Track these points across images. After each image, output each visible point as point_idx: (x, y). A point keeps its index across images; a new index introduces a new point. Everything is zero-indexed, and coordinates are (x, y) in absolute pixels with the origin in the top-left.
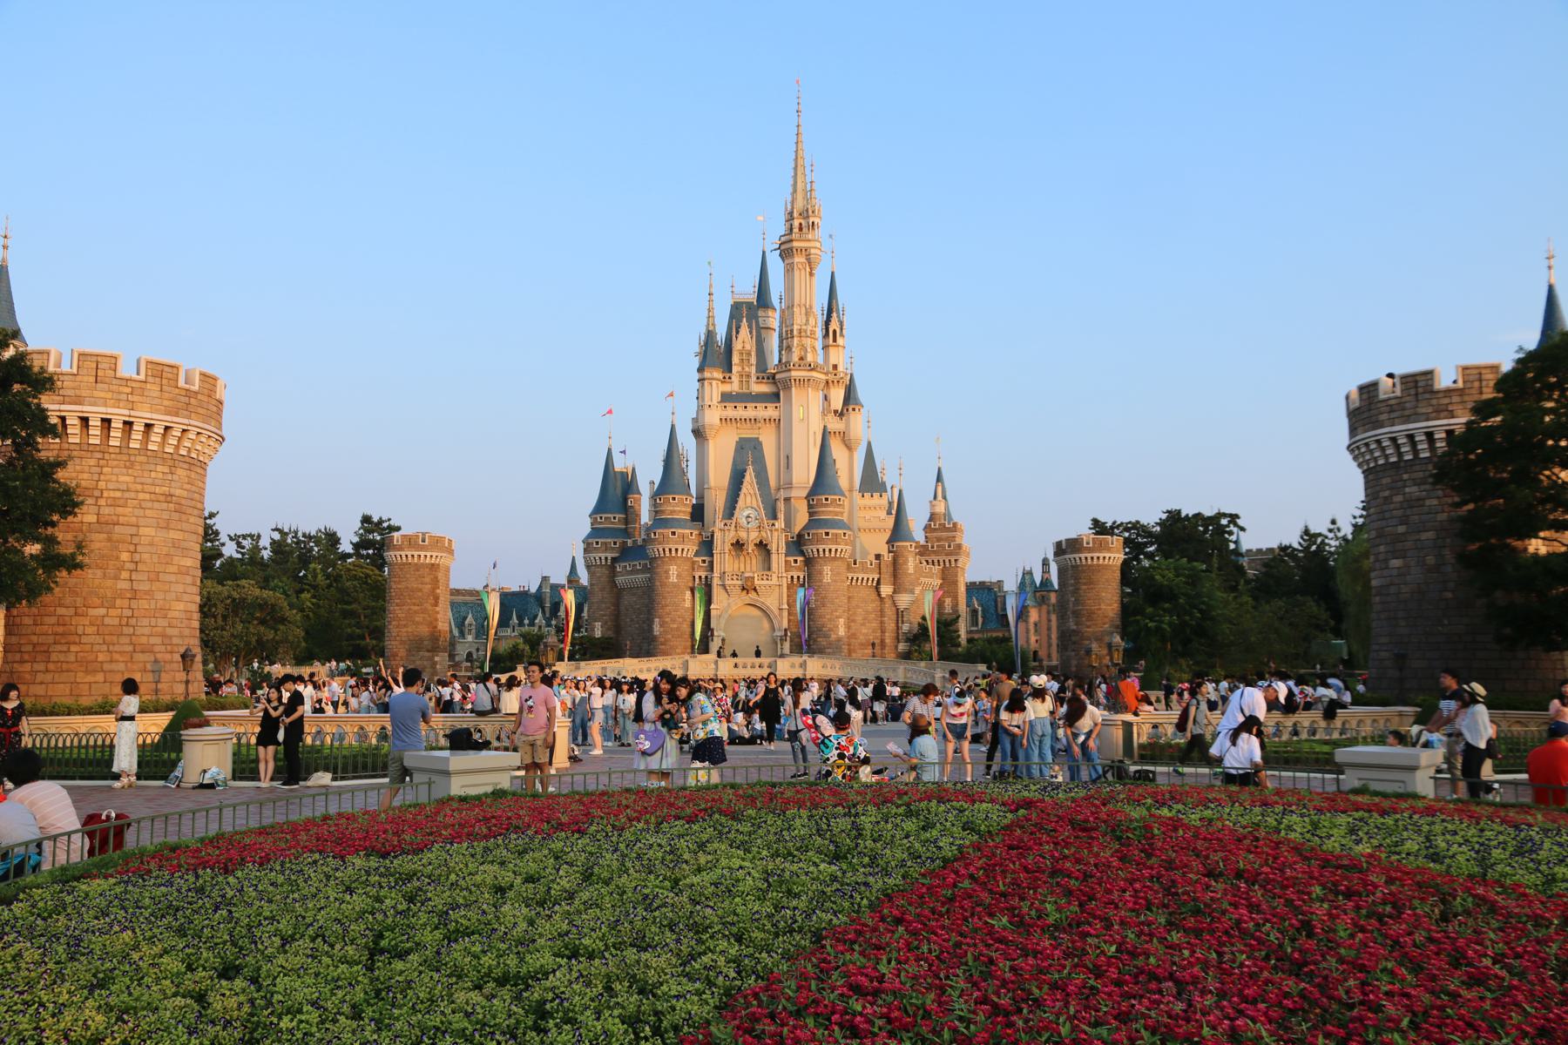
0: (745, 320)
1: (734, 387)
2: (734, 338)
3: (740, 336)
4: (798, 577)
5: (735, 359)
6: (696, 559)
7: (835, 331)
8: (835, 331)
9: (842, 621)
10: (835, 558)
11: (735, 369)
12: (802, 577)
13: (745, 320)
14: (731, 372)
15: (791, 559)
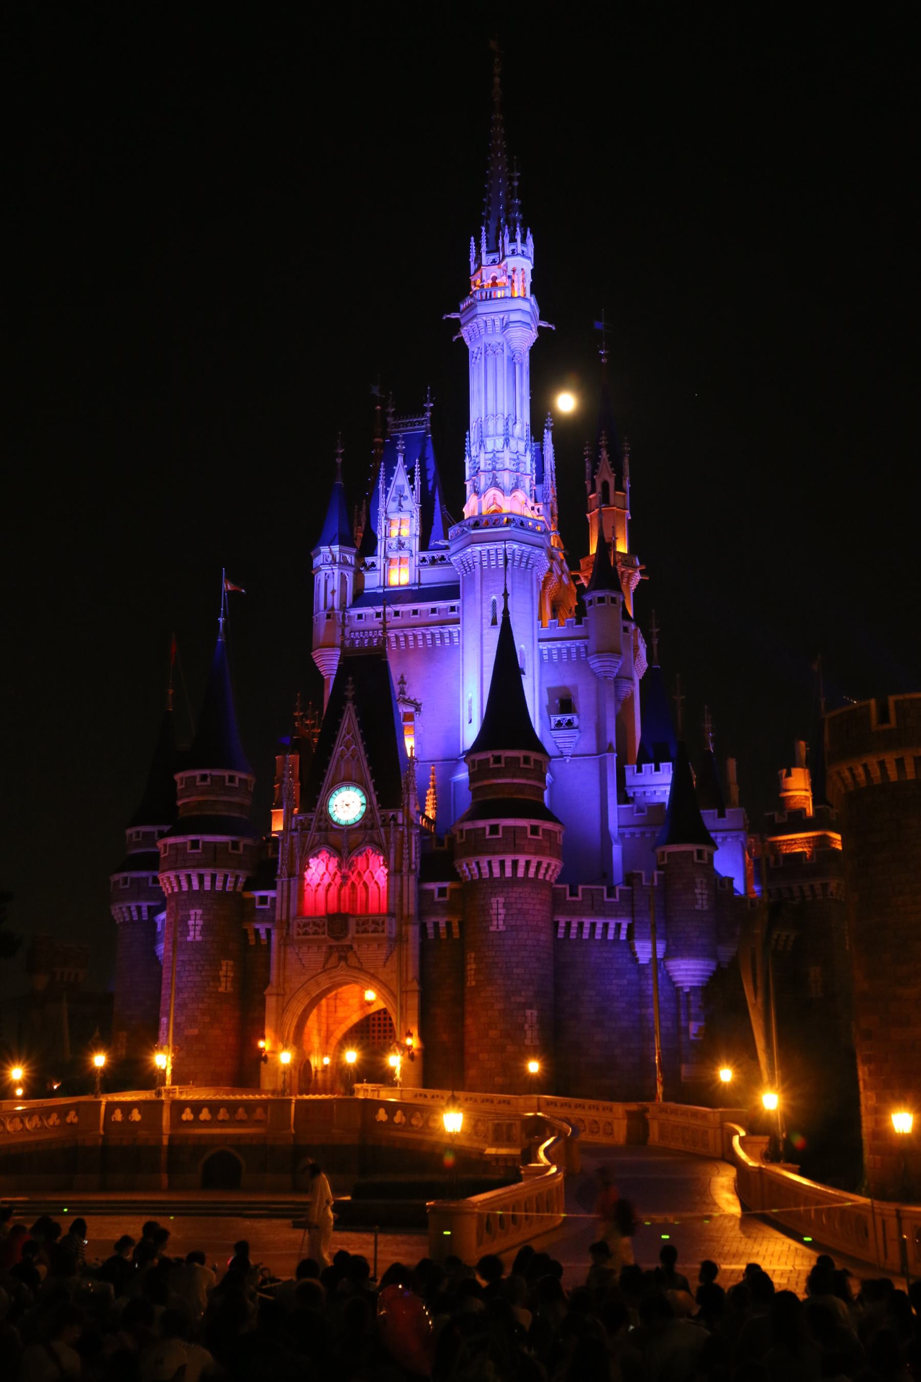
0: (400, 460)
3: (392, 491)
4: (449, 924)
6: (247, 895)
7: (605, 485)
8: (605, 485)
9: (532, 1014)
10: (514, 879)
12: (455, 924)
13: (400, 460)
15: (433, 886)
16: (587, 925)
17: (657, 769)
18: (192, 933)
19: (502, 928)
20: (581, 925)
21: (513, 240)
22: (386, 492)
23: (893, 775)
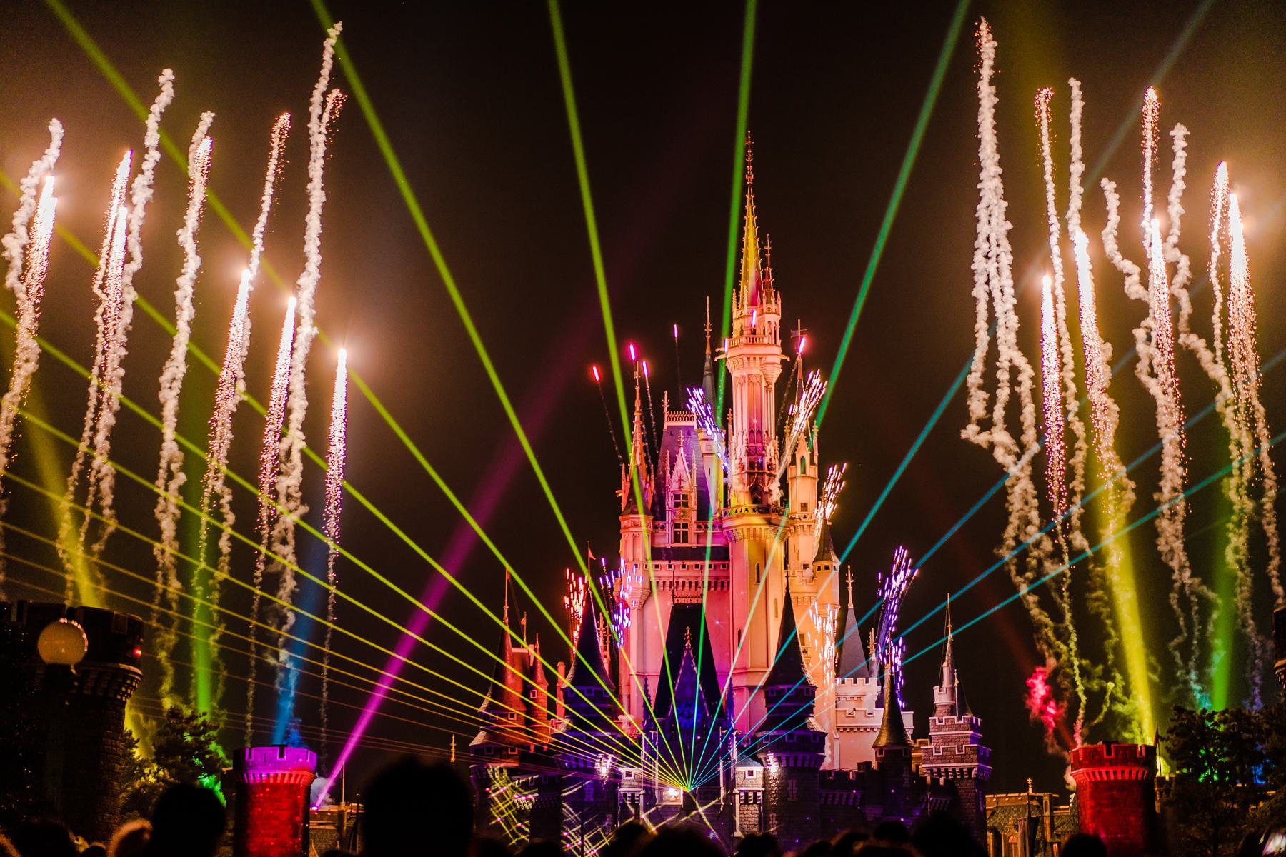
1: (666, 541)
2: (669, 474)
5: (670, 503)
8: (802, 458)
11: (669, 516)
14: (663, 519)
16: (838, 796)
17: (855, 682)
18: (587, 796)
19: (795, 799)
20: (834, 796)
21: (769, 301)
22: (671, 474)
23: (1112, 777)
